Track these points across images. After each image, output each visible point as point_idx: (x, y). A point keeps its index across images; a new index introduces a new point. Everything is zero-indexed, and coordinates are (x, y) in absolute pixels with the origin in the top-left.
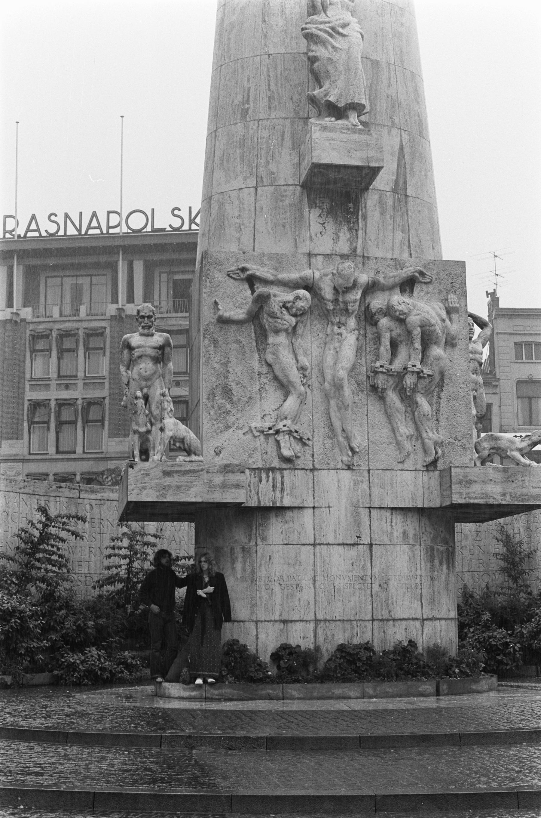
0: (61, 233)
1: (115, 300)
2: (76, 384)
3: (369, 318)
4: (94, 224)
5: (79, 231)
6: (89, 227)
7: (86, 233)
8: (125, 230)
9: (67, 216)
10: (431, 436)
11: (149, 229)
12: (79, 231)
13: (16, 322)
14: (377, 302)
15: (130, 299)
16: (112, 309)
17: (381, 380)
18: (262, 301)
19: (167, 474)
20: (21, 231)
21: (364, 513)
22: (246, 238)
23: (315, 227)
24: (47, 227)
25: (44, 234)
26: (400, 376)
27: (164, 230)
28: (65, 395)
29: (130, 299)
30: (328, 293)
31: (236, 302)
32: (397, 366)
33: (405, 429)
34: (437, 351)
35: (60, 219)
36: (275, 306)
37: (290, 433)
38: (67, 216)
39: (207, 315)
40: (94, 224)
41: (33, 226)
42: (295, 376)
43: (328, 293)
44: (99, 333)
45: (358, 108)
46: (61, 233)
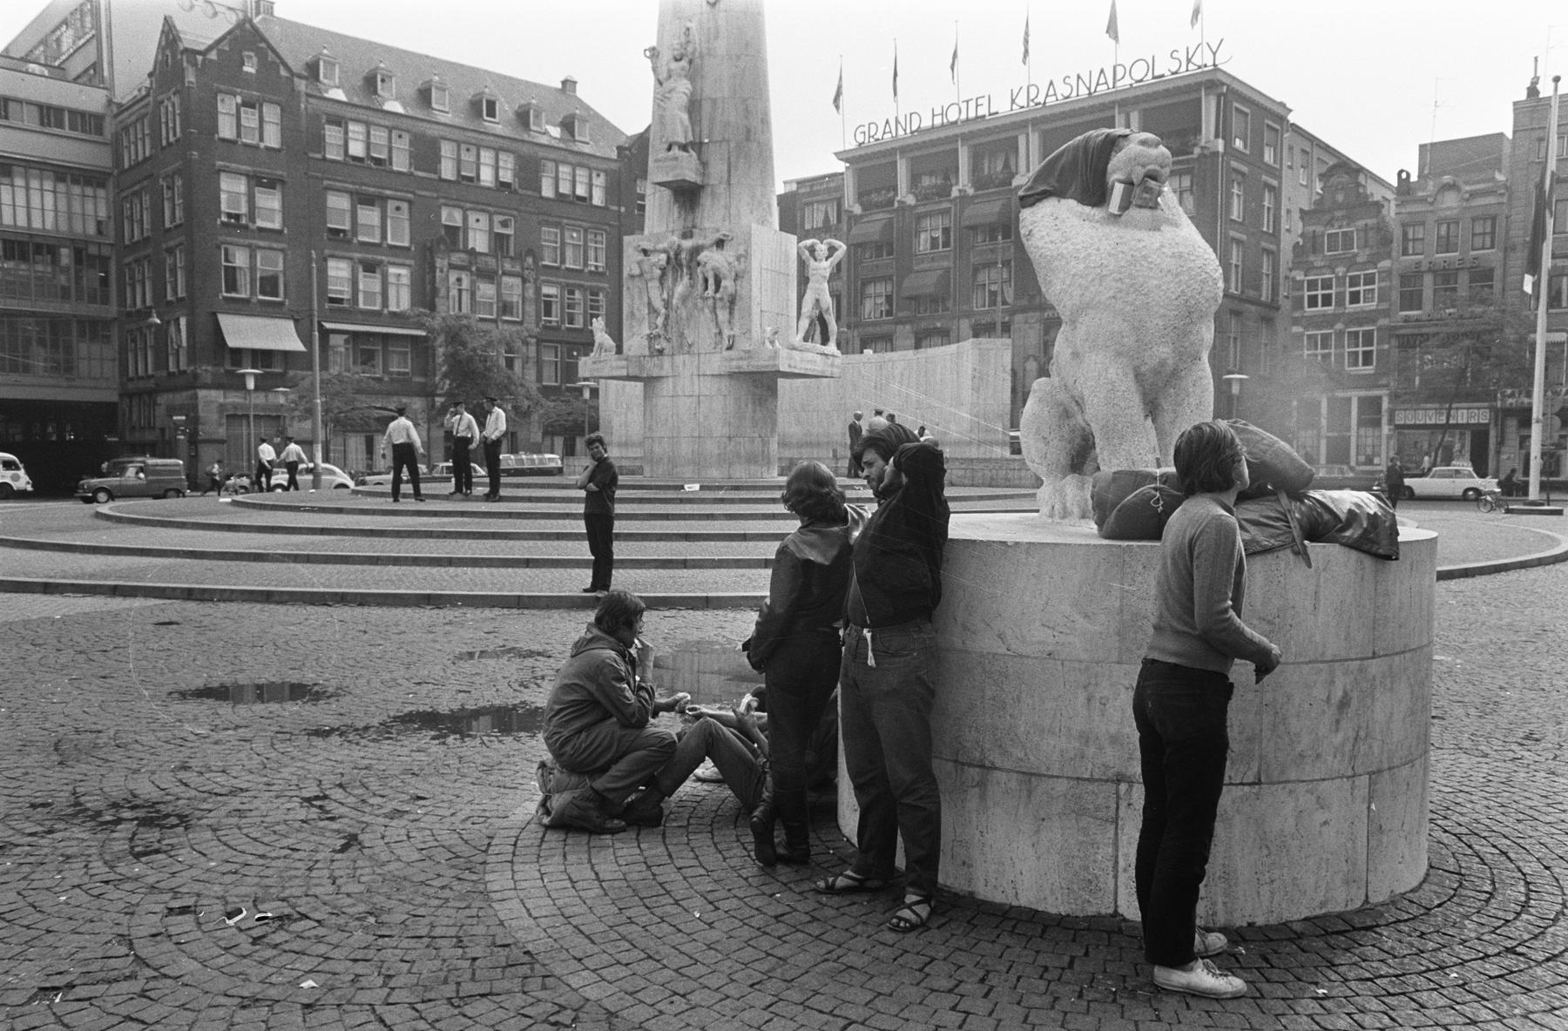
4: (1102, 80)
20: (1041, 99)
35: (1073, 81)
40: (1102, 80)
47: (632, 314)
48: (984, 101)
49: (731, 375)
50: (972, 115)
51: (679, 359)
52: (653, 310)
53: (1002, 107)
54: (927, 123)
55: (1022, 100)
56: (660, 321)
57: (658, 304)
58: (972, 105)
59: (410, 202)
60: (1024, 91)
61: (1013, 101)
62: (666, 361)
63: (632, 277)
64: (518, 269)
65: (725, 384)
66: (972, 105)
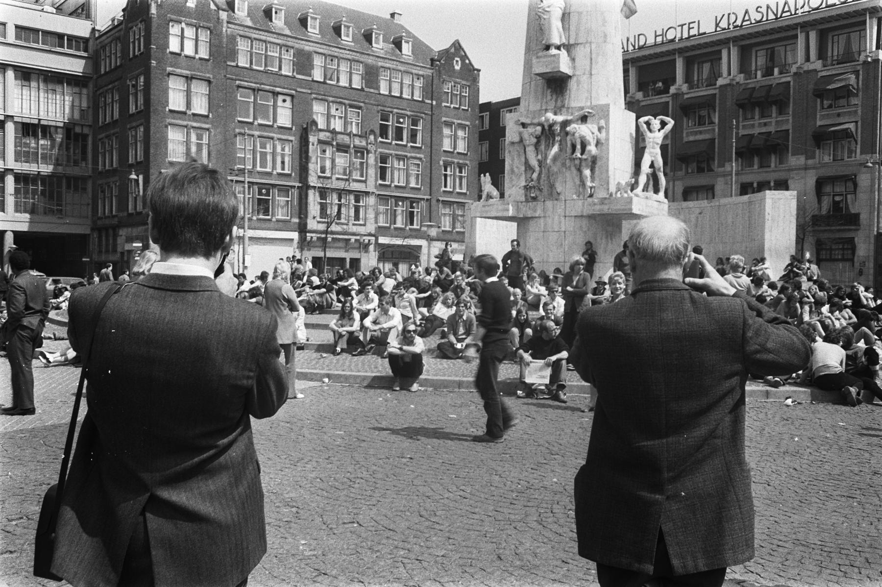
0: (764, 19)
2: (771, 122)
5: (776, 15)
6: (783, 12)
7: (781, 17)
8: (806, 9)
9: (768, 7)
11: (824, 5)
12: (776, 15)
13: (733, 85)
19: (484, 206)
20: (739, 23)
21: (563, 218)
23: (549, 97)
24: (755, 16)
25: (753, 22)
27: (835, 5)
29: (808, 59)
37: (534, 187)
38: (768, 7)
41: (747, 18)
46: (764, 19)
47: (512, 171)
48: (695, 25)
49: (591, 217)
50: (685, 35)
51: (549, 204)
52: (528, 167)
53: (708, 27)
54: (651, 41)
55: (724, 24)
56: (535, 176)
57: (534, 162)
58: (686, 28)
59: (292, 96)
60: (726, 17)
61: (717, 25)
62: (539, 206)
63: (513, 143)
64: (364, 143)
65: (585, 223)
66: (686, 28)
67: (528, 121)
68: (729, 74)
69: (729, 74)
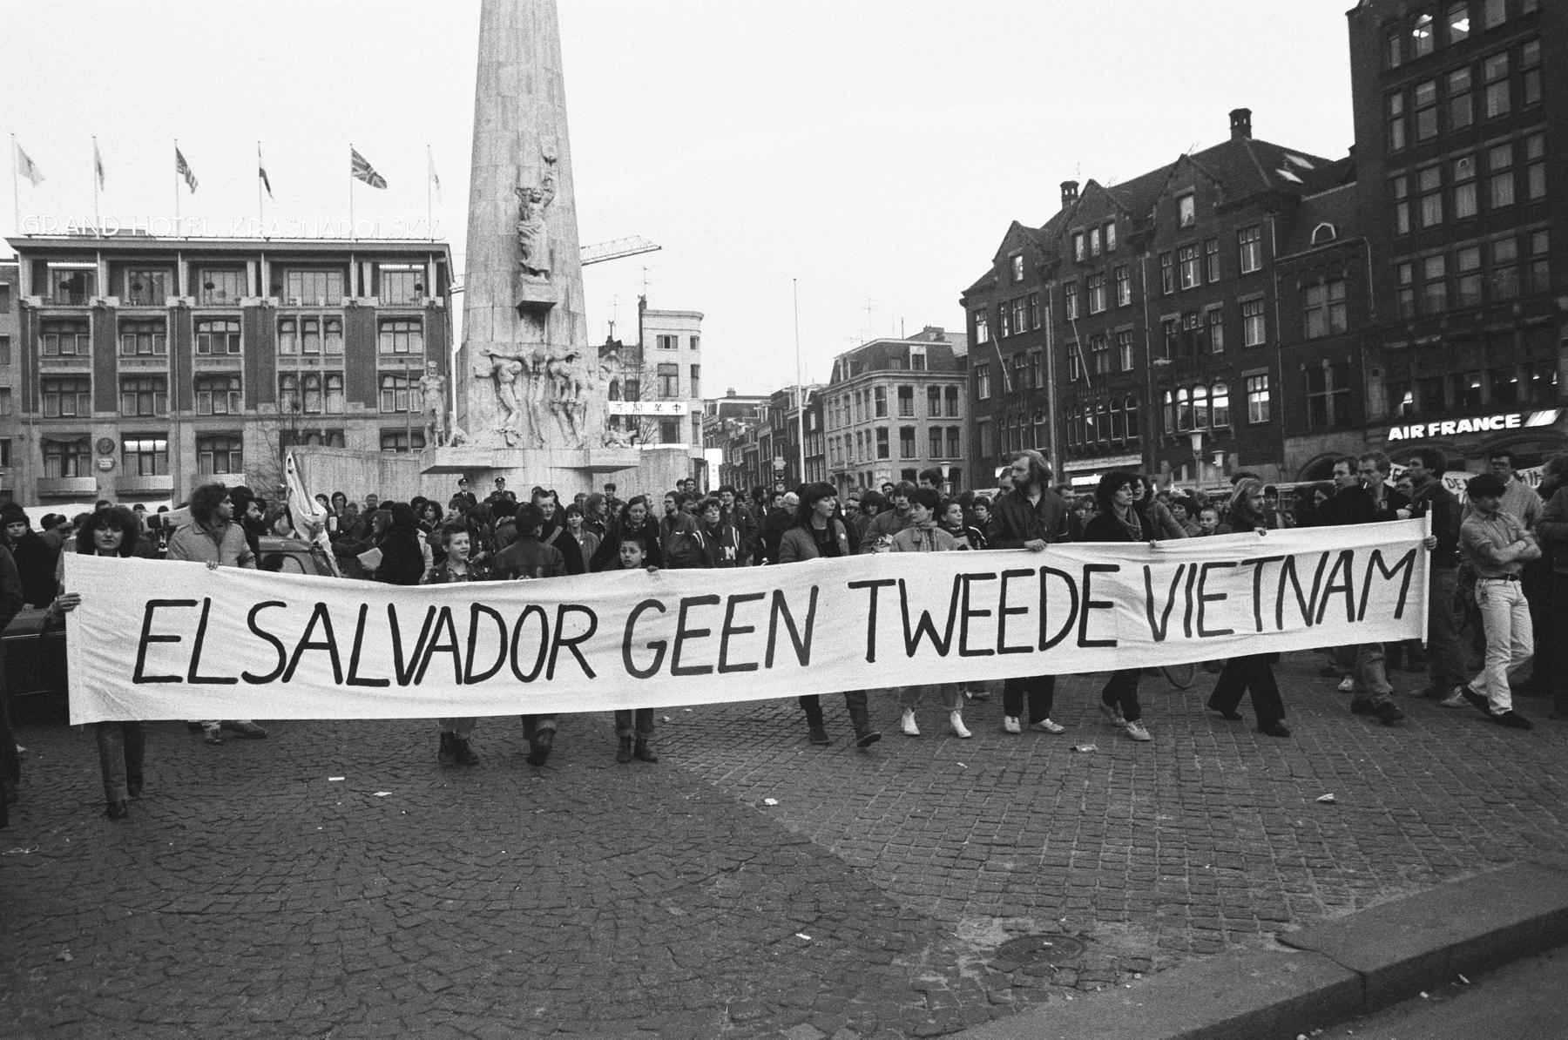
1: (348, 292)
3: (550, 375)
10: (580, 434)
14: (554, 367)
15: (361, 293)
16: (345, 301)
17: (556, 407)
18: (497, 369)
22: (489, 333)
26: (566, 404)
28: (308, 368)
29: (361, 293)
30: (530, 364)
31: (485, 367)
32: (564, 399)
33: (568, 430)
34: (583, 392)
36: (503, 370)
39: (471, 375)
42: (513, 404)
43: (530, 364)
44: (337, 319)
45: (545, 272)
67: (497, 352)
68: (259, 293)
69: (259, 293)
